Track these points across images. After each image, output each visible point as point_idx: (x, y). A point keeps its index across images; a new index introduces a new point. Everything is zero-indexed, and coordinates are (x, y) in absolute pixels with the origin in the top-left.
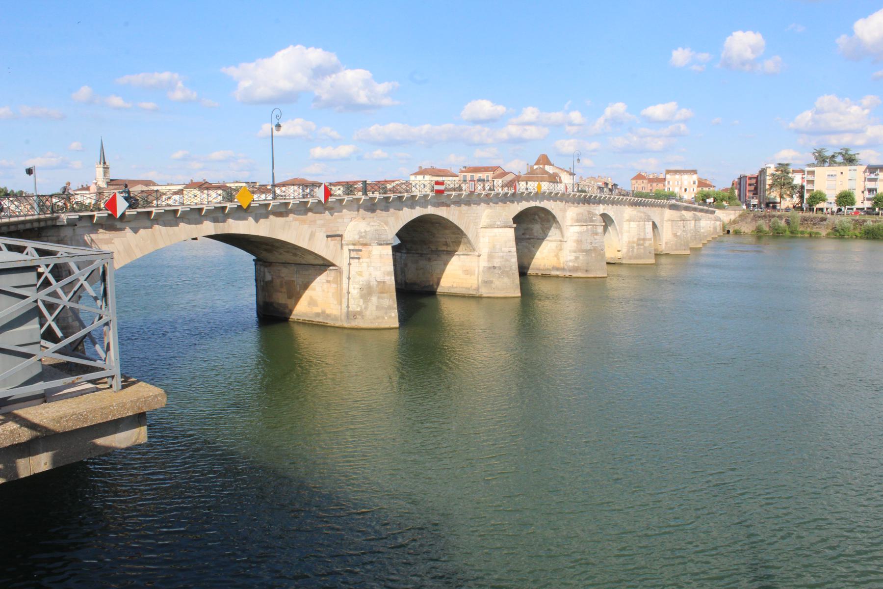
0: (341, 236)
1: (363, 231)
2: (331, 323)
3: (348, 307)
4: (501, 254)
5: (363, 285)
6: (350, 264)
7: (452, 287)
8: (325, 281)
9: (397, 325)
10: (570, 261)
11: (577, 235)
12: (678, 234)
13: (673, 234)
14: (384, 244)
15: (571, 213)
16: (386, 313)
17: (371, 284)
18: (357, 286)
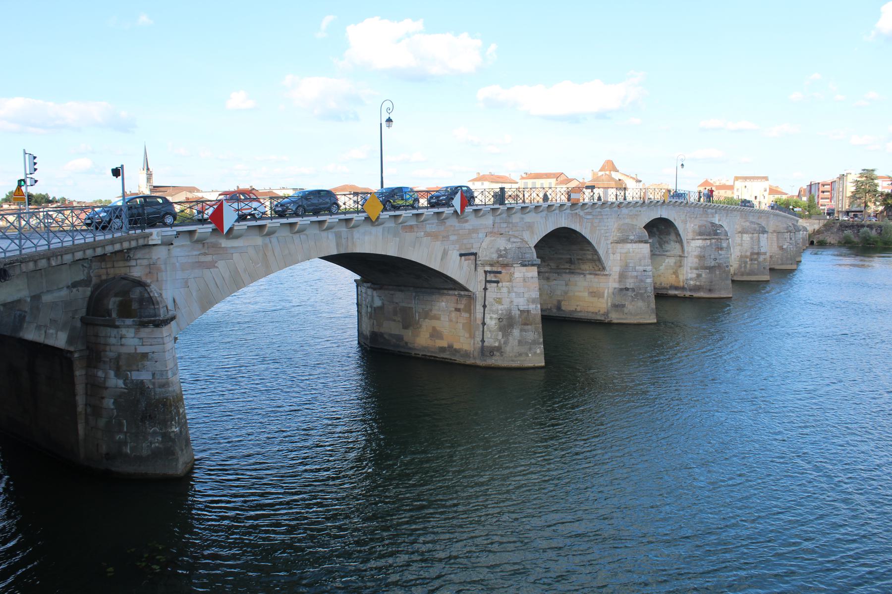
0: (475, 254)
1: (502, 248)
2: (459, 359)
3: (483, 341)
4: (635, 274)
5: (502, 314)
6: (485, 289)
7: (576, 311)
8: (454, 309)
9: (543, 364)
10: (691, 279)
11: (700, 250)
12: (785, 247)
13: (778, 247)
14: (529, 265)
15: (692, 225)
16: (530, 349)
17: (513, 314)
18: (495, 316)
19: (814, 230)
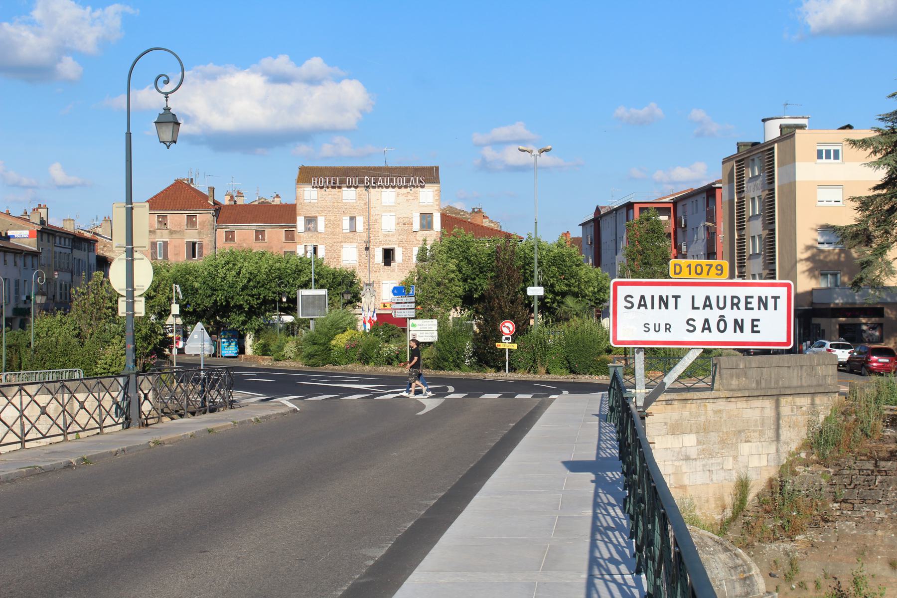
19: (743, 486)
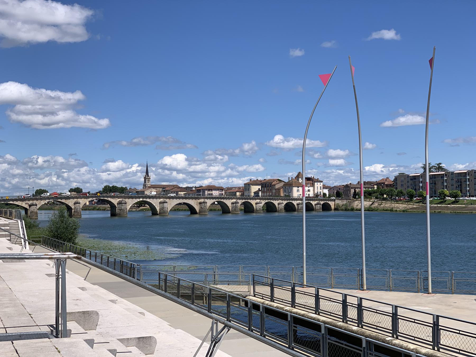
12: (202, 207)
13: (201, 207)
